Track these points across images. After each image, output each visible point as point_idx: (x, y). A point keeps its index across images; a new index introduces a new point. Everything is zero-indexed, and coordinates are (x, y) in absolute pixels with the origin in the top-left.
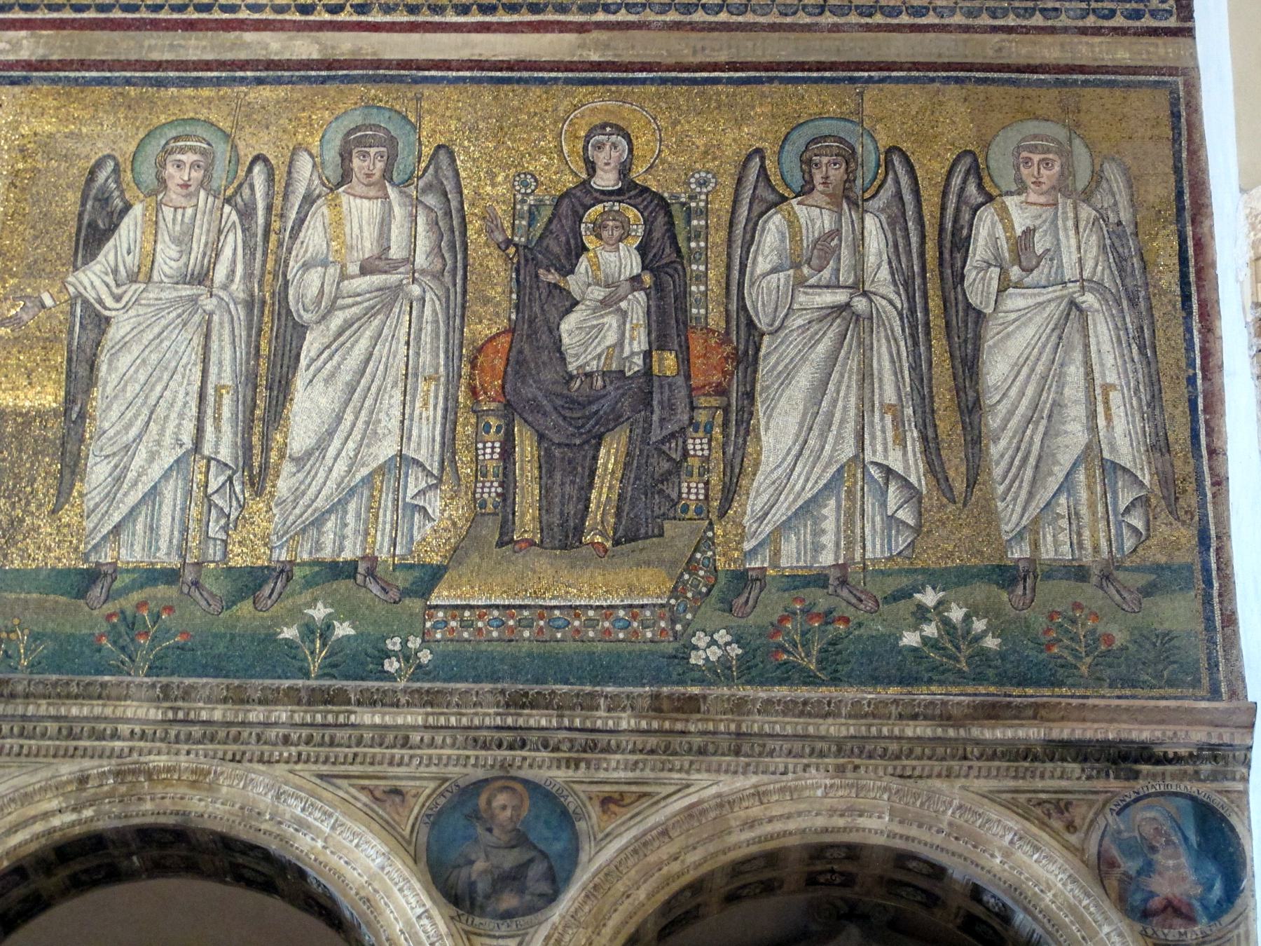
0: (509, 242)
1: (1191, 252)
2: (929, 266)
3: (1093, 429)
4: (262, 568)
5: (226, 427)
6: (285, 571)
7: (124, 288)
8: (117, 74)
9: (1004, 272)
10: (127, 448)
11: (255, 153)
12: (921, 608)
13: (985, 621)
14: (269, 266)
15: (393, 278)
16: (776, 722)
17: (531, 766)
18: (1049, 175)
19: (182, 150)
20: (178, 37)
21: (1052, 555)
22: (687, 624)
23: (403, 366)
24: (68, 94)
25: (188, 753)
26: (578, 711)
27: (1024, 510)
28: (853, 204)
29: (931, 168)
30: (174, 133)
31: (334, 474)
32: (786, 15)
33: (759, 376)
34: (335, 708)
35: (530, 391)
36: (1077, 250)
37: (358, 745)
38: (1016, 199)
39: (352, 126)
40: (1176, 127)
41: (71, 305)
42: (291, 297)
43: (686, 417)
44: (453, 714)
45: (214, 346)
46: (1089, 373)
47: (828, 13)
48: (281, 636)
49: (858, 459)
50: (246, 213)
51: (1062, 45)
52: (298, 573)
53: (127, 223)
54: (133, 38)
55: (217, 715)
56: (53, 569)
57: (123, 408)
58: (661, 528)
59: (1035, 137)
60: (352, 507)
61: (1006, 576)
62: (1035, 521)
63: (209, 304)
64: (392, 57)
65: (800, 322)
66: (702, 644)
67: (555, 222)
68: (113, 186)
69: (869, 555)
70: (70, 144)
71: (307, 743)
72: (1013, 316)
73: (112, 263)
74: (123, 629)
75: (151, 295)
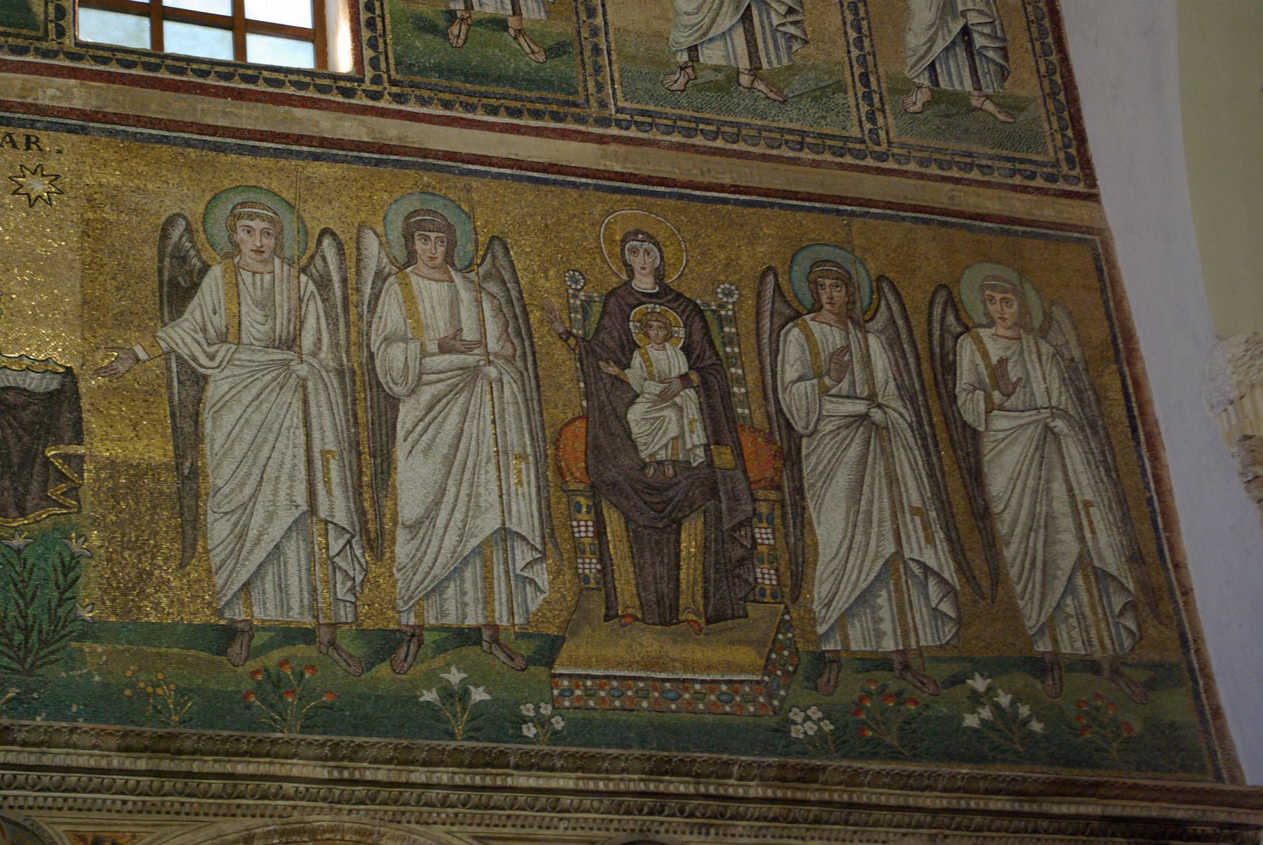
0: (569, 334)
1: (1131, 390)
2: (927, 385)
3: (1082, 539)
4: (393, 631)
5: (337, 491)
6: (416, 634)
7: (215, 348)
8: (175, 134)
9: (988, 398)
10: (244, 506)
11: (323, 227)
12: (974, 692)
13: (1027, 707)
14: (353, 336)
15: (470, 359)
16: (882, 794)
17: (667, 831)
18: (1012, 312)
19: (251, 217)
20: (229, 104)
21: (1068, 650)
22: (783, 700)
23: (492, 442)
24: (128, 149)
25: (350, 812)
26: (712, 780)
27: (1041, 609)
28: (861, 326)
29: (917, 298)
30: (239, 199)
31: (446, 544)
32: (772, 148)
33: (805, 473)
34: (494, 771)
35: (611, 474)
36: (1043, 381)
37: (511, 808)
38: (987, 330)
39: (412, 210)
40: (1101, 280)
41: (165, 359)
42: (378, 370)
43: (749, 508)
44: (600, 779)
45: (313, 411)
46: (1070, 490)
48: (422, 699)
49: (899, 553)
50: (323, 284)
51: (1000, 198)
52: (428, 638)
53: (207, 283)
54: (185, 100)
55: (382, 774)
56: (190, 624)
57: (234, 467)
58: (745, 610)
59: (994, 278)
60: (468, 574)
61: (1040, 667)
62: (1051, 619)
63: (303, 370)
64: (438, 148)
65: (829, 428)
66: (799, 719)
67: (607, 318)
68: (188, 245)
69: (923, 643)
70: (136, 198)
71: (464, 805)
72: (1001, 435)
73: (199, 321)
74: (269, 687)
75: (244, 357)
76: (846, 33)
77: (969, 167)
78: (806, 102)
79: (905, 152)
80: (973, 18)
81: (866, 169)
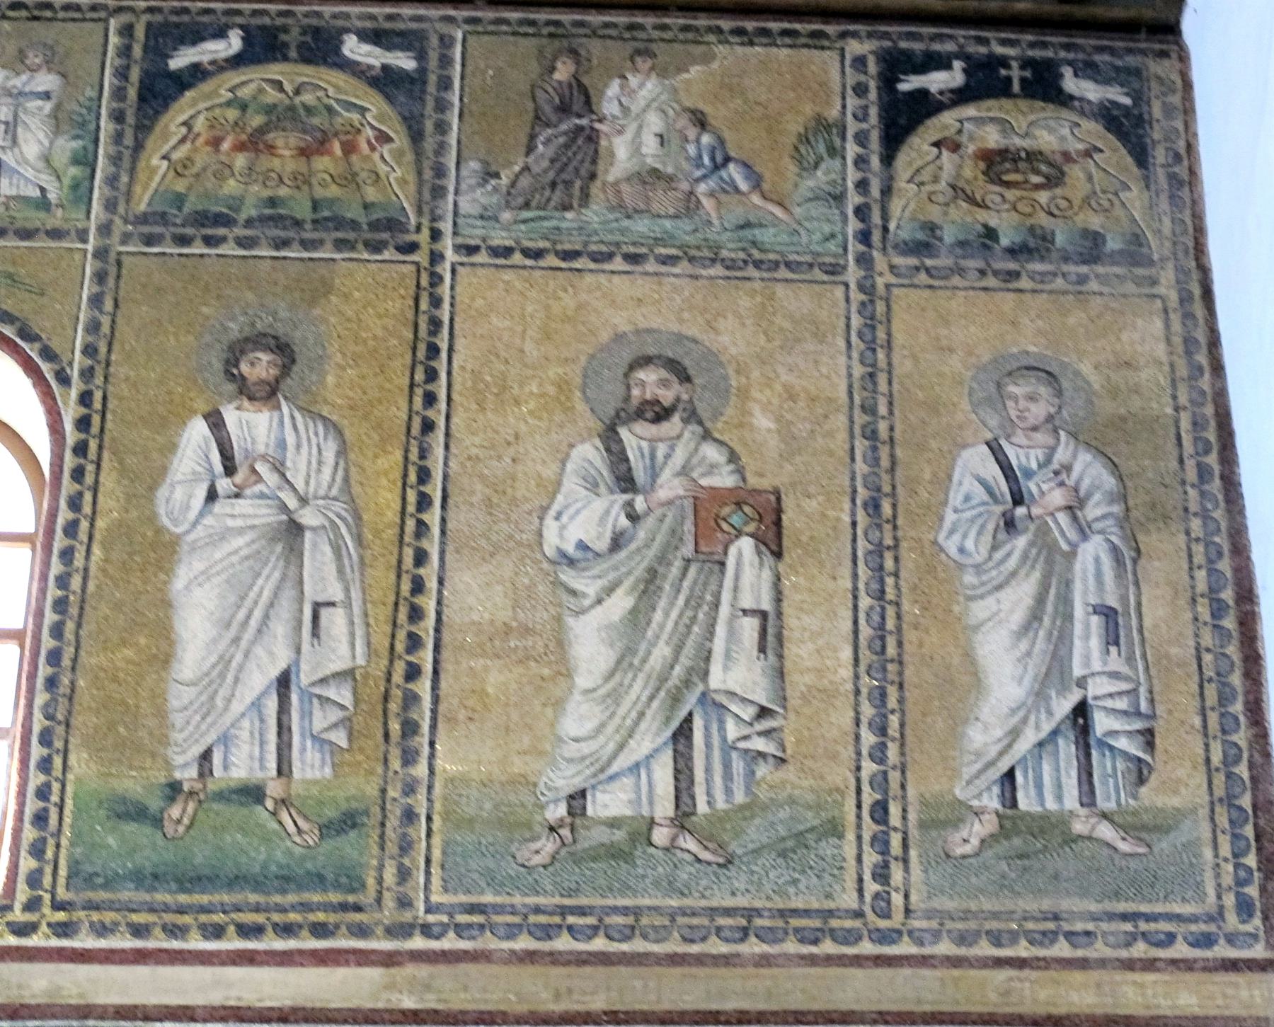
32: (692, 941)
47: (753, 939)
51: (1098, 986)
76: (857, 738)
77: (1049, 937)
78: (767, 859)
79: (934, 924)
80: (1098, 687)
81: (858, 961)
